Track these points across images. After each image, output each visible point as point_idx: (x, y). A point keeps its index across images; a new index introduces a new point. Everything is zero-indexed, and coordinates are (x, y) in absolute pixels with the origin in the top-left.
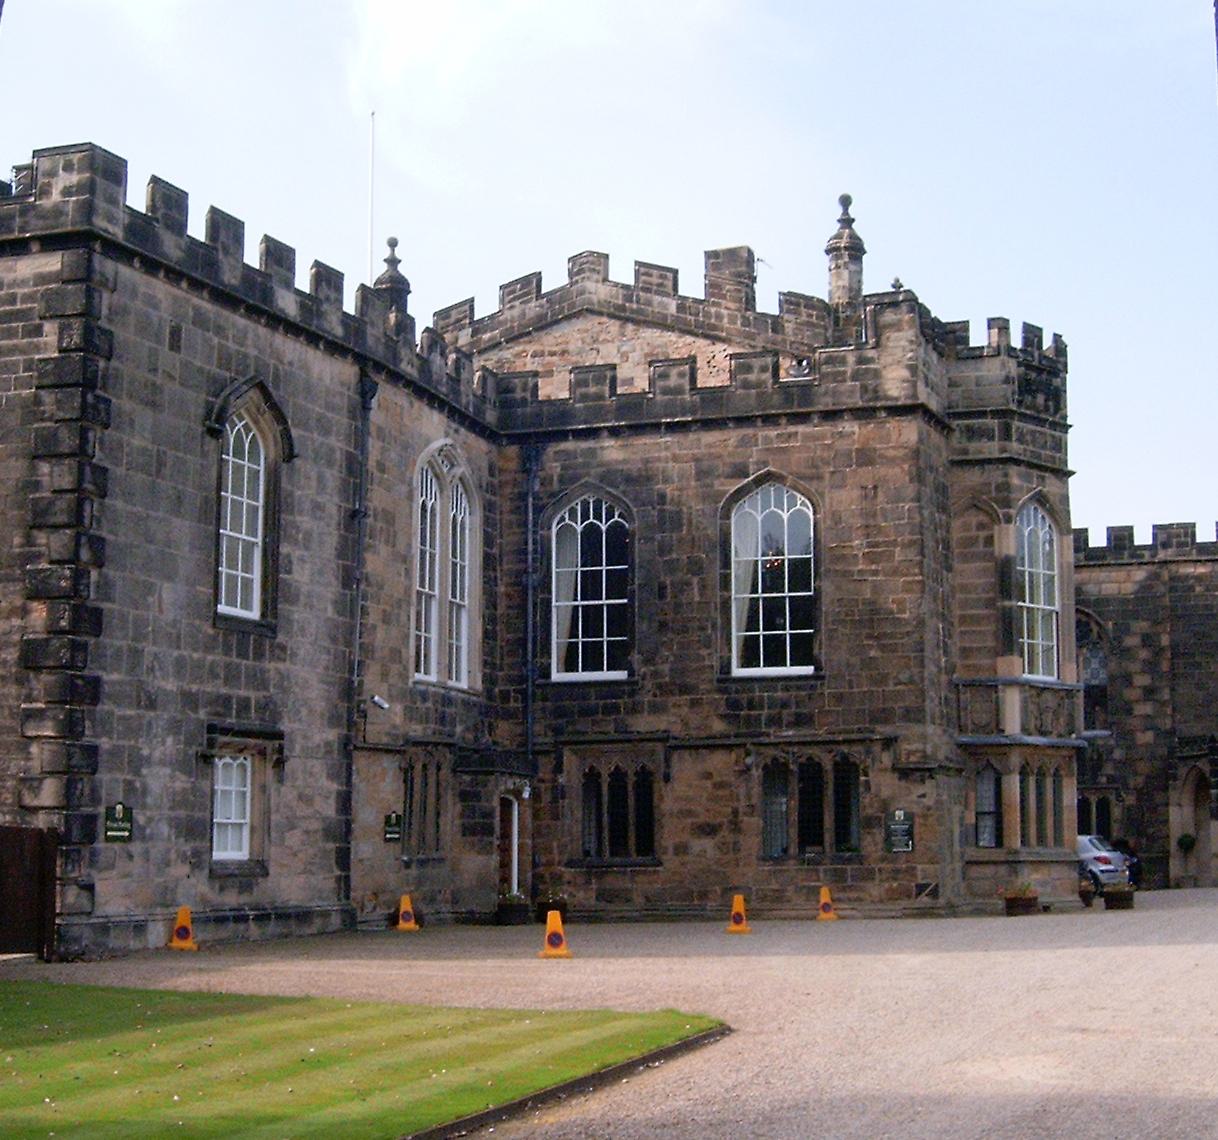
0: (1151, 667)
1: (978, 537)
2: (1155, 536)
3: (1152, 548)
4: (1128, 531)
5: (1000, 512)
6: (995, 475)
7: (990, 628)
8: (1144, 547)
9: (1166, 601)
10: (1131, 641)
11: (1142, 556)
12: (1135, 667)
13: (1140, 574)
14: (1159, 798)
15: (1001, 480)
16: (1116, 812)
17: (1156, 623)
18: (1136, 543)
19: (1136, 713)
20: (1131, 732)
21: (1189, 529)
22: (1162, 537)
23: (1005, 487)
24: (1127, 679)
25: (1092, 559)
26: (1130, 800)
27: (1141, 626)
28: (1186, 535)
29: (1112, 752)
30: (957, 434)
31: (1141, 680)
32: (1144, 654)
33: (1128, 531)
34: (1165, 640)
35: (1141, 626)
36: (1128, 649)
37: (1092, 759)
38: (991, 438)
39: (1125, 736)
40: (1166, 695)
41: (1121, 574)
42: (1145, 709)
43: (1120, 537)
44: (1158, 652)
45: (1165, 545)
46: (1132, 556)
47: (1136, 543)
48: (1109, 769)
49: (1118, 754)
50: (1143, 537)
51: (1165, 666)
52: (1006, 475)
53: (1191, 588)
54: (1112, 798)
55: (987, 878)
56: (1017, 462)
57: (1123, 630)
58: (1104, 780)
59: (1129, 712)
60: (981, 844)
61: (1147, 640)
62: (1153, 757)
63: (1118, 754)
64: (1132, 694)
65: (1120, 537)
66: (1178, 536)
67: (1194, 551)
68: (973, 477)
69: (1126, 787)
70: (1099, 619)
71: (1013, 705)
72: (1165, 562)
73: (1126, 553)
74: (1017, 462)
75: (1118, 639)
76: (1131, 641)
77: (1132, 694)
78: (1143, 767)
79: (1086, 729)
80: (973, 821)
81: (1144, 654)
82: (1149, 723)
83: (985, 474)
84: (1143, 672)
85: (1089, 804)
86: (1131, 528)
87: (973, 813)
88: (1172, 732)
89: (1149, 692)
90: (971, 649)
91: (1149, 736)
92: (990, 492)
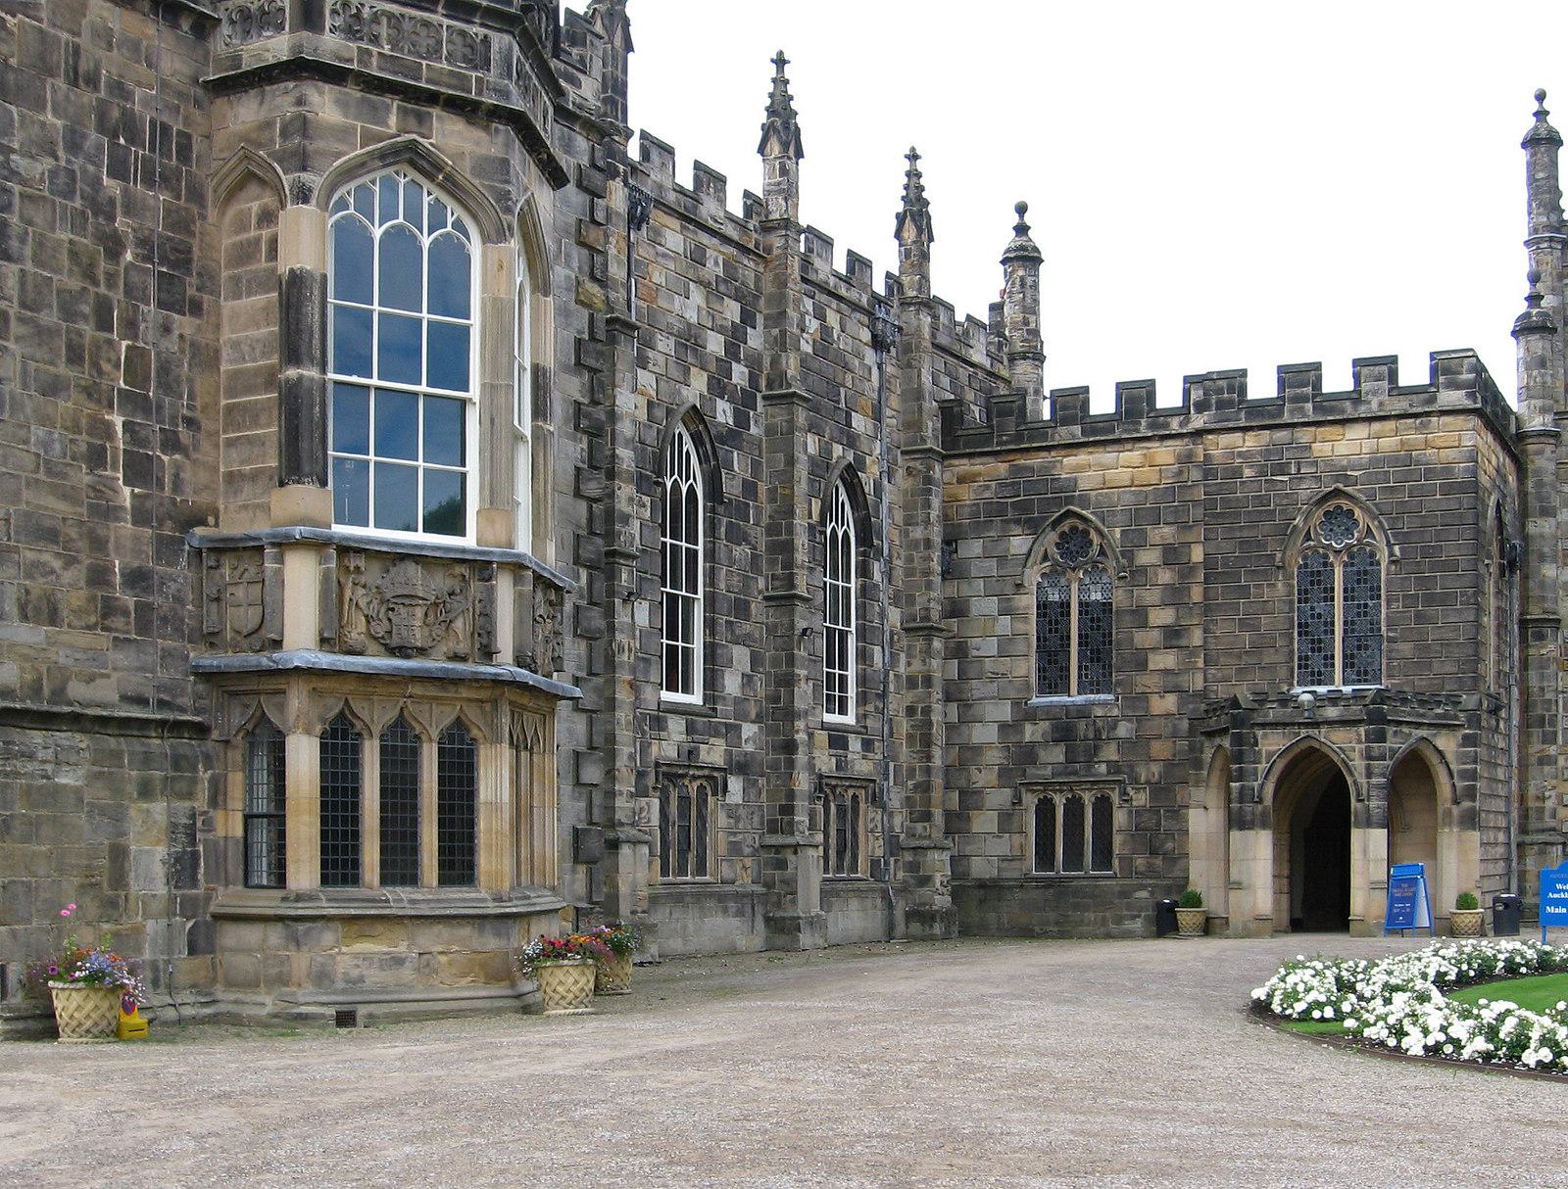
0: (1175, 596)
1: (258, 240)
2: (1186, 393)
3: (1183, 412)
4: (1148, 387)
5: (287, 180)
6: (281, 101)
7: (270, 430)
8: (1172, 413)
9: (1200, 494)
10: (1147, 557)
11: (1166, 426)
12: (1151, 596)
13: (1165, 453)
14: (1180, 794)
15: (291, 111)
16: (1120, 818)
17: (1184, 527)
18: (1159, 405)
19: (1151, 666)
20: (1144, 697)
21: (1236, 380)
22: (1196, 394)
23: (302, 126)
24: (1140, 615)
25: (1094, 432)
26: (1141, 799)
27: (1166, 533)
28: (1231, 390)
29: (1114, 727)
30: (225, 29)
31: (1163, 617)
32: (1165, 576)
33: (1148, 387)
34: (1197, 554)
35: (1166, 533)
36: (1143, 570)
37: (1086, 739)
38: (280, 28)
39: (1136, 702)
40: (1196, 638)
41: (1133, 456)
42: (1166, 660)
43: (1136, 397)
44: (1187, 570)
45: (1201, 407)
46: (1151, 426)
47: (1159, 405)
48: (1110, 753)
49: (1124, 730)
50: (1169, 397)
51: (1197, 594)
52: (300, 102)
53: (1237, 473)
54: (1115, 798)
55: (249, 951)
56: (332, 74)
57: (1136, 539)
58: (1103, 768)
59: (1142, 665)
60: (255, 881)
61: (1172, 555)
62: (1175, 735)
63: (1124, 730)
64: (1145, 638)
65: (1136, 397)
66: (1220, 391)
67: (1243, 415)
68: (245, 113)
69: (1135, 780)
70: (1100, 524)
71: (301, 582)
72: (1199, 434)
73: (1143, 422)
74: (332, 74)
75: (1128, 555)
76: (1147, 557)
77: (1145, 638)
78: (1160, 749)
79: (1042, 692)
80: (239, 832)
81: (1165, 576)
82: (1171, 683)
83: (265, 106)
84: (1164, 605)
85: (1082, 806)
86: (1152, 383)
87: (239, 817)
88: (1203, 694)
89: (1173, 635)
90: (241, 475)
91: (1170, 703)
92: (272, 141)
